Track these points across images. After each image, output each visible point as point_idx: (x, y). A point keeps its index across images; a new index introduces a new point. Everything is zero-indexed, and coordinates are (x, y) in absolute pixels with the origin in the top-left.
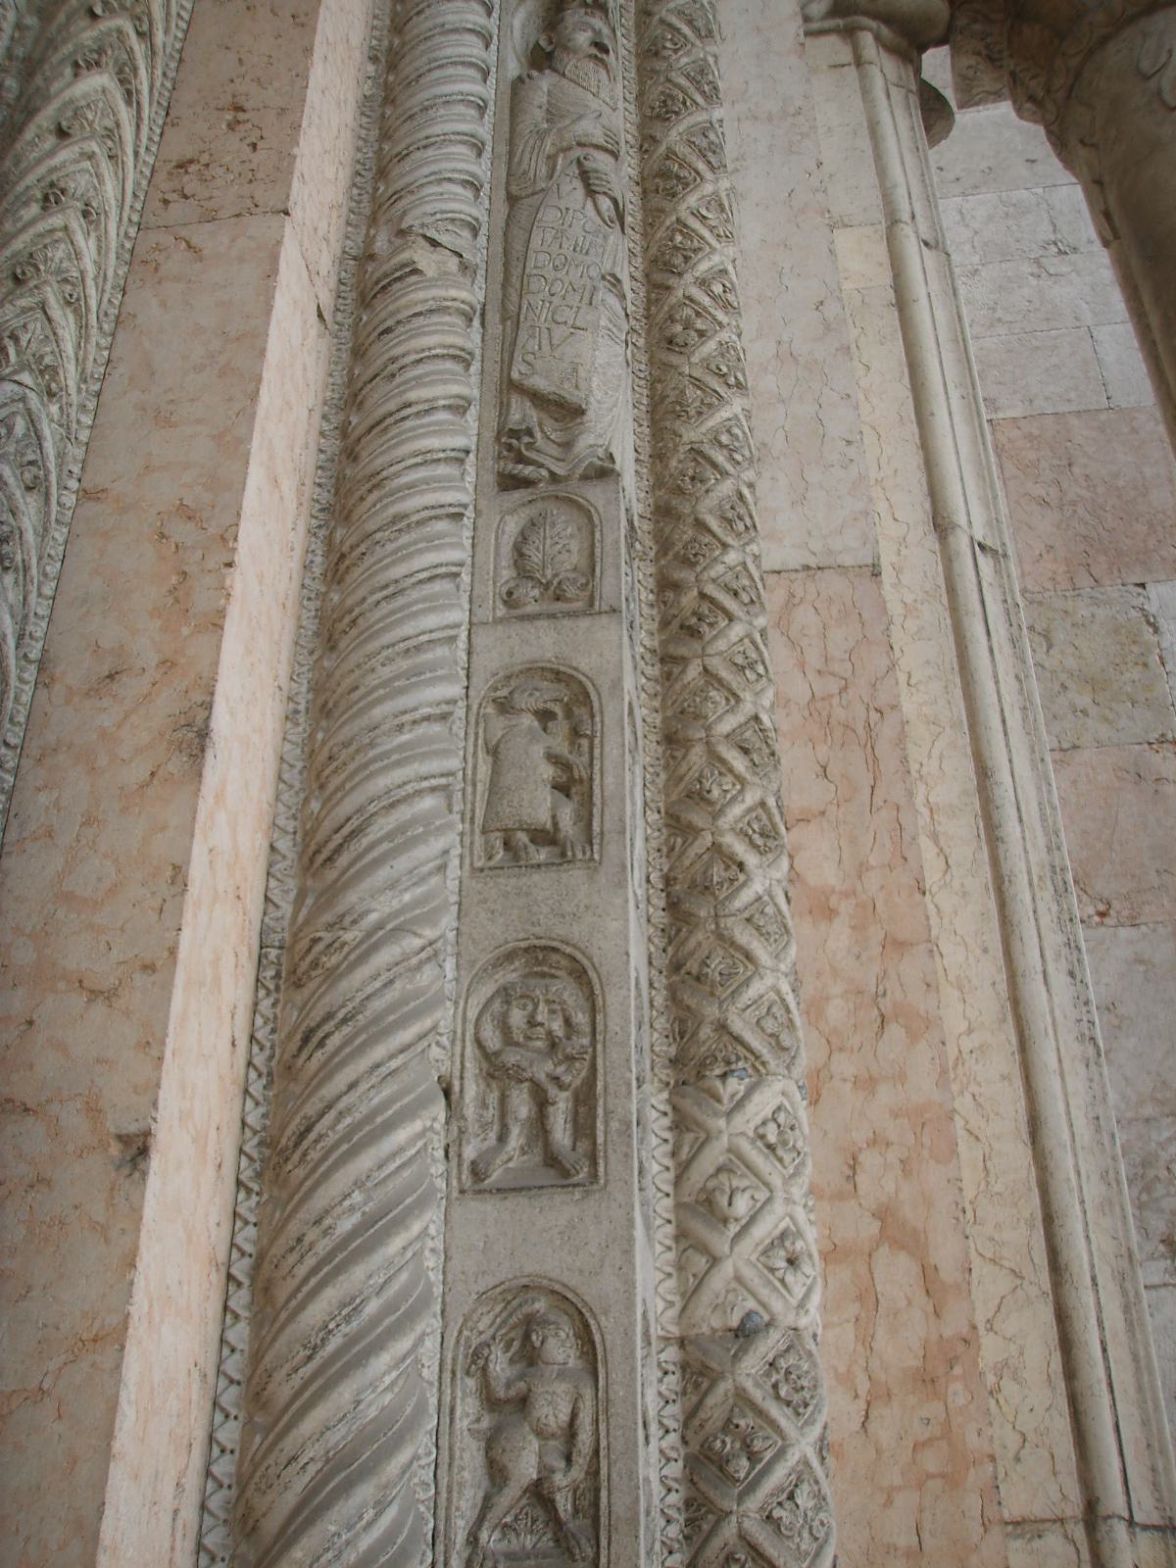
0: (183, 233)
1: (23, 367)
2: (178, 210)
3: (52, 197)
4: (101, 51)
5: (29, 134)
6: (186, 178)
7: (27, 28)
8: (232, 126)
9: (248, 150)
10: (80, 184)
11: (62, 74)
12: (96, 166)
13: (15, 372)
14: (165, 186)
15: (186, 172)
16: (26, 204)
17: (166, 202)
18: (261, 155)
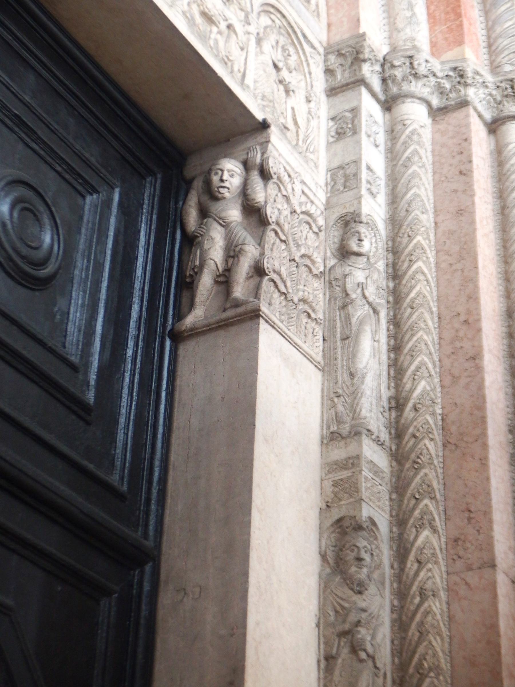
0: (463, 576)
1: (430, 669)
2: (459, 564)
3: (422, 593)
4: (422, 518)
5: (409, 565)
6: (459, 548)
7: (394, 500)
8: (469, 519)
9: (476, 532)
10: (429, 585)
11: (412, 532)
12: (432, 573)
13: (429, 672)
14: (452, 552)
15: (458, 545)
16: (415, 598)
17: (453, 559)
18: (481, 537)
